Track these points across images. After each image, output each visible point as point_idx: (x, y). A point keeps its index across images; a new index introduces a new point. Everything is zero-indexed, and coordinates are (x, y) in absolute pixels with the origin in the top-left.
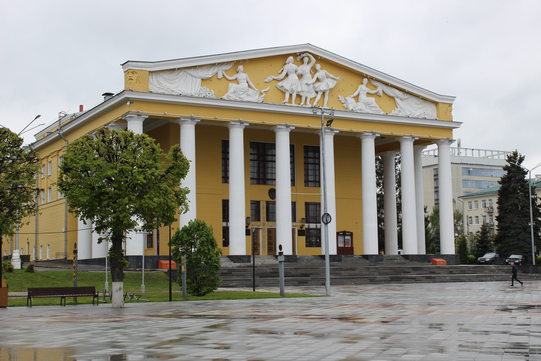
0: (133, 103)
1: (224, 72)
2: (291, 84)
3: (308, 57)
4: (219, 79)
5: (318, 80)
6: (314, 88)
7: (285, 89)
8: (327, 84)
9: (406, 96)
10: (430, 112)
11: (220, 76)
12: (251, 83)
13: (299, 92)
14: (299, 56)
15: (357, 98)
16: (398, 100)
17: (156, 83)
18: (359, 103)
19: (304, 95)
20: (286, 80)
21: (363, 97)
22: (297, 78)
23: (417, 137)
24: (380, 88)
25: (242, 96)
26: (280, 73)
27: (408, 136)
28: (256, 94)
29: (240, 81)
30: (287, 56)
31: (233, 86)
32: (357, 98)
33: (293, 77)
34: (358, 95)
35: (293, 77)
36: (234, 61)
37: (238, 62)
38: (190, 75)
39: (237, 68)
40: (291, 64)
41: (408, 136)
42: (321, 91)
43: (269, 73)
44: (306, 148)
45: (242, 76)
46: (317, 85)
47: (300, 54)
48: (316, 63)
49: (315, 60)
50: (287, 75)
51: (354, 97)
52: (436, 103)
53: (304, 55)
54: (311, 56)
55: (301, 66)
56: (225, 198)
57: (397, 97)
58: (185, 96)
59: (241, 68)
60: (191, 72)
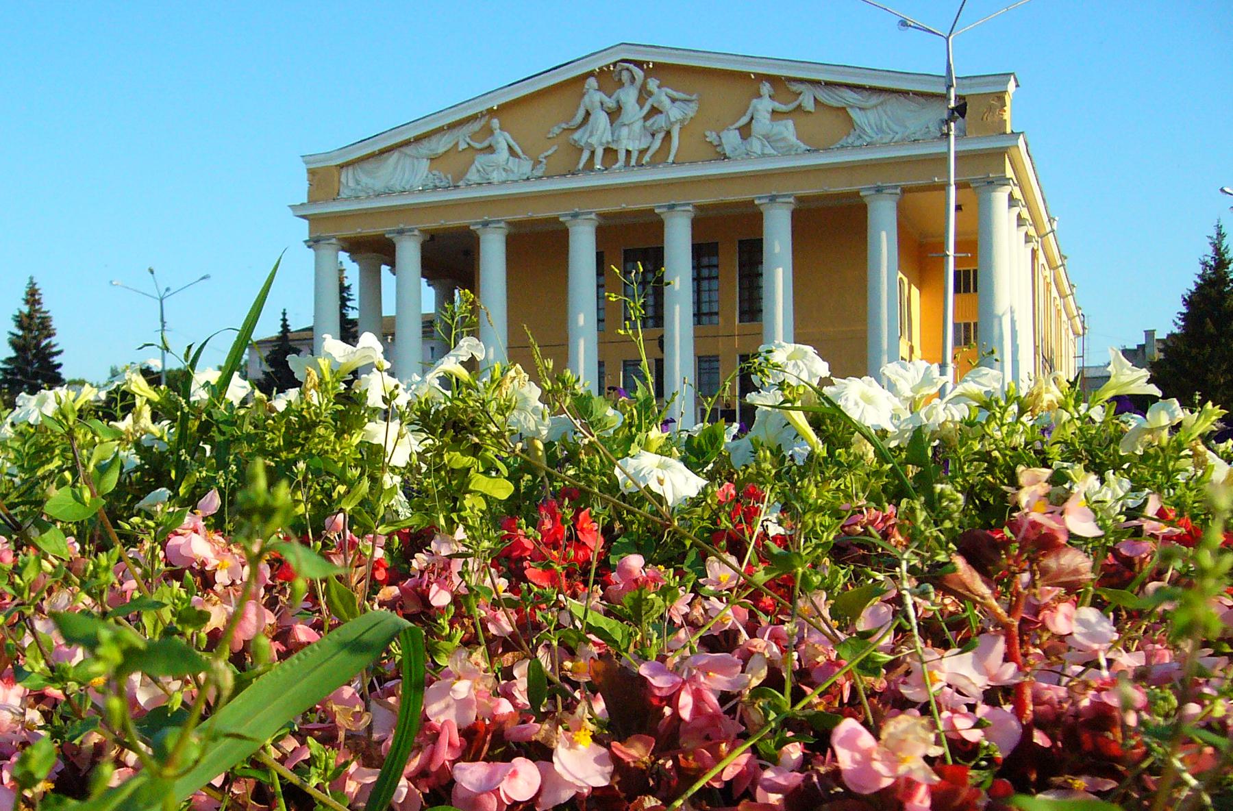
1: (468, 140)
2: (600, 131)
5: (655, 111)
9: (875, 100)
13: (608, 143)
16: (855, 115)
21: (763, 122)
31: (481, 160)
46: (648, 123)
48: (646, 78)
50: (588, 114)
54: (631, 66)
57: (852, 107)
59: (495, 123)
60: (407, 150)
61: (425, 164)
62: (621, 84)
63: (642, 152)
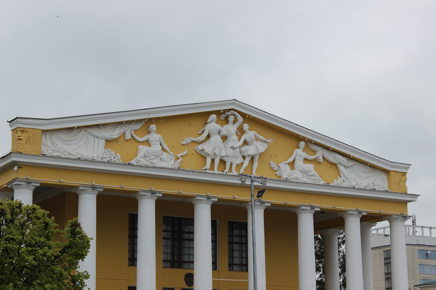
0: (21, 168)
1: (133, 133)
3: (234, 115)
4: (127, 140)
5: (246, 143)
6: (241, 152)
7: (206, 154)
8: (257, 147)
9: (351, 163)
10: (380, 182)
11: (128, 137)
12: (165, 146)
13: (223, 157)
14: (223, 115)
15: (292, 165)
16: (341, 168)
17: (50, 144)
18: (294, 171)
19: (228, 161)
20: (207, 143)
21: (300, 164)
22: (220, 140)
23: (364, 212)
24: (320, 153)
25: (154, 161)
26: (201, 134)
27: (354, 211)
28: (171, 159)
29: (153, 143)
30: (209, 113)
31: (143, 149)
32: (292, 165)
33: (216, 139)
34: (294, 161)
35: (216, 139)
36: (145, 119)
37: (150, 121)
38: (92, 135)
39: (149, 127)
40: (213, 124)
41: (354, 211)
42: (249, 155)
43: (187, 135)
44: (231, 224)
45: (155, 137)
46: (244, 149)
47: (225, 111)
48: (243, 122)
49: (242, 119)
50: (209, 136)
51: (288, 164)
52: (387, 172)
53: (229, 113)
54: (237, 114)
55: (226, 126)
56: (131, 285)
57: (340, 164)
58: (86, 160)
59: (153, 127)
60: (94, 131)
61: (103, 142)
62: (226, 120)
63: (240, 166)
